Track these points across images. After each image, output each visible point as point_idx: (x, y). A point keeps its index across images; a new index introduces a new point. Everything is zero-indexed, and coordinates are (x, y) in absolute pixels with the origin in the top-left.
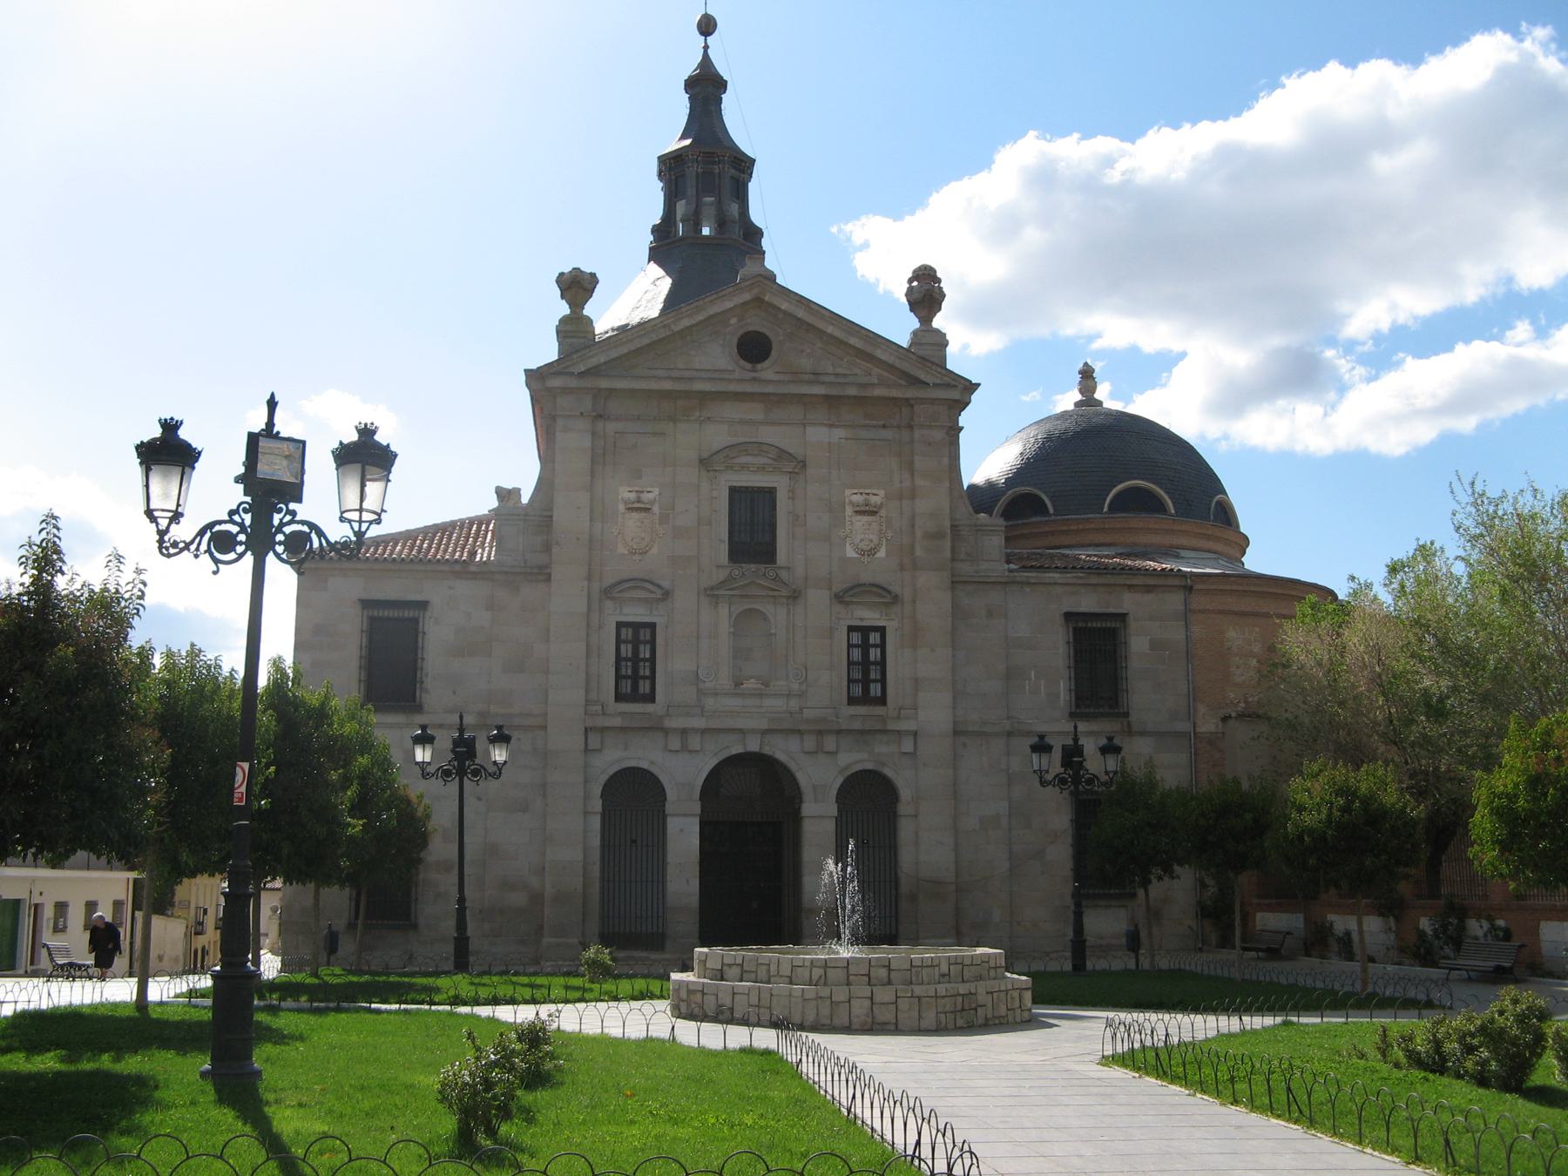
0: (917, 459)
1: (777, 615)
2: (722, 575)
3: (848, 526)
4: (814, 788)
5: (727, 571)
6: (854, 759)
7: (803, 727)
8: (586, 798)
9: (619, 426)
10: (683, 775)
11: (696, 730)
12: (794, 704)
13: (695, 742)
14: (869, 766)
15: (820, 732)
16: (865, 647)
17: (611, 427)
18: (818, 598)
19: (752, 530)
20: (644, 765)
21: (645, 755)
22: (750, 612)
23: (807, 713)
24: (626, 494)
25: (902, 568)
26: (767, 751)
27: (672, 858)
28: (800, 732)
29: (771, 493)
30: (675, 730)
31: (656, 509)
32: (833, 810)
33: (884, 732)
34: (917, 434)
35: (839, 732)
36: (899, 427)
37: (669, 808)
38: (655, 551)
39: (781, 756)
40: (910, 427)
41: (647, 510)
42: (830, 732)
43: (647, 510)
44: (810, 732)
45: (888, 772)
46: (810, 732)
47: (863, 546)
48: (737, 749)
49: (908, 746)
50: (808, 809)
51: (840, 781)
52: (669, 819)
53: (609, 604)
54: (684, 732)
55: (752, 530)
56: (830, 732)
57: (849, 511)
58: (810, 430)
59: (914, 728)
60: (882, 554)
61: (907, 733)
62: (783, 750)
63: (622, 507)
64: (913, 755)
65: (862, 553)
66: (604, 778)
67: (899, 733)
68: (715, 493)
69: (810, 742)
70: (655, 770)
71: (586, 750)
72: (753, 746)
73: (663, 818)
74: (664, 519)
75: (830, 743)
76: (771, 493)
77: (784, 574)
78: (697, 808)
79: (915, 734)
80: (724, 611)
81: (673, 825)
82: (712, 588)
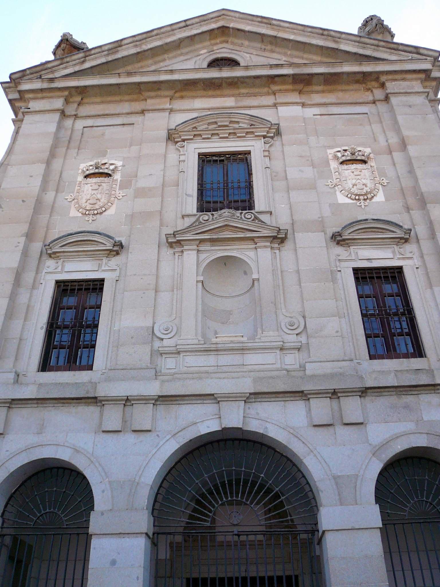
0: (400, 118)
1: (260, 259)
2: (188, 222)
3: (335, 176)
4: (336, 478)
5: (193, 219)
9: (89, 122)
11: (144, 400)
12: (291, 360)
13: (143, 416)
15: (335, 394)
16: (379, 298)
17: (80, 124)
18: (311, 248)
19: (224, 185)
20: (64, 455)
22: (226, 262)
23: (310, 369)
24: (86, 165)
25: (408, 209)
26: (254, 426)
29: (243, 158)
30: (114, 400)
31: (117, 176)
32: (373, 515)
34: (394, 100)
35: (364, 392)
36: (374, 102)
37: (96, 523)
38: (112, 211)
39: (276, 433)
40: (387, 99)
41: (108, 175)
42: (349, 392)
43: (108, 175)
44: (319, 394)
46: (319, 394)
47: (355, 190)
48: (209, 426)
50: (329, 517)
51: (377, 467)
52: (95, 543)
53: (50, 263)
54: (127, 401)
55: (224, 185)
56: (349, 392)
57: (334, 165)
58: (280, 108)
60: (380, 197)
62: (278, 423)
63: (80, 178)
65: (357, 197)
68: (182, 158)
69: (321, 408)
70: (80, 464)
72: (234, 417)
73: (84, 538)
74: (125, 185)
75: (352, 408)
76: (243, 158)
77: (264, 218)
78: (143, 522)
80: (190, 257)
81: (100, 550)
82: (174, 235)
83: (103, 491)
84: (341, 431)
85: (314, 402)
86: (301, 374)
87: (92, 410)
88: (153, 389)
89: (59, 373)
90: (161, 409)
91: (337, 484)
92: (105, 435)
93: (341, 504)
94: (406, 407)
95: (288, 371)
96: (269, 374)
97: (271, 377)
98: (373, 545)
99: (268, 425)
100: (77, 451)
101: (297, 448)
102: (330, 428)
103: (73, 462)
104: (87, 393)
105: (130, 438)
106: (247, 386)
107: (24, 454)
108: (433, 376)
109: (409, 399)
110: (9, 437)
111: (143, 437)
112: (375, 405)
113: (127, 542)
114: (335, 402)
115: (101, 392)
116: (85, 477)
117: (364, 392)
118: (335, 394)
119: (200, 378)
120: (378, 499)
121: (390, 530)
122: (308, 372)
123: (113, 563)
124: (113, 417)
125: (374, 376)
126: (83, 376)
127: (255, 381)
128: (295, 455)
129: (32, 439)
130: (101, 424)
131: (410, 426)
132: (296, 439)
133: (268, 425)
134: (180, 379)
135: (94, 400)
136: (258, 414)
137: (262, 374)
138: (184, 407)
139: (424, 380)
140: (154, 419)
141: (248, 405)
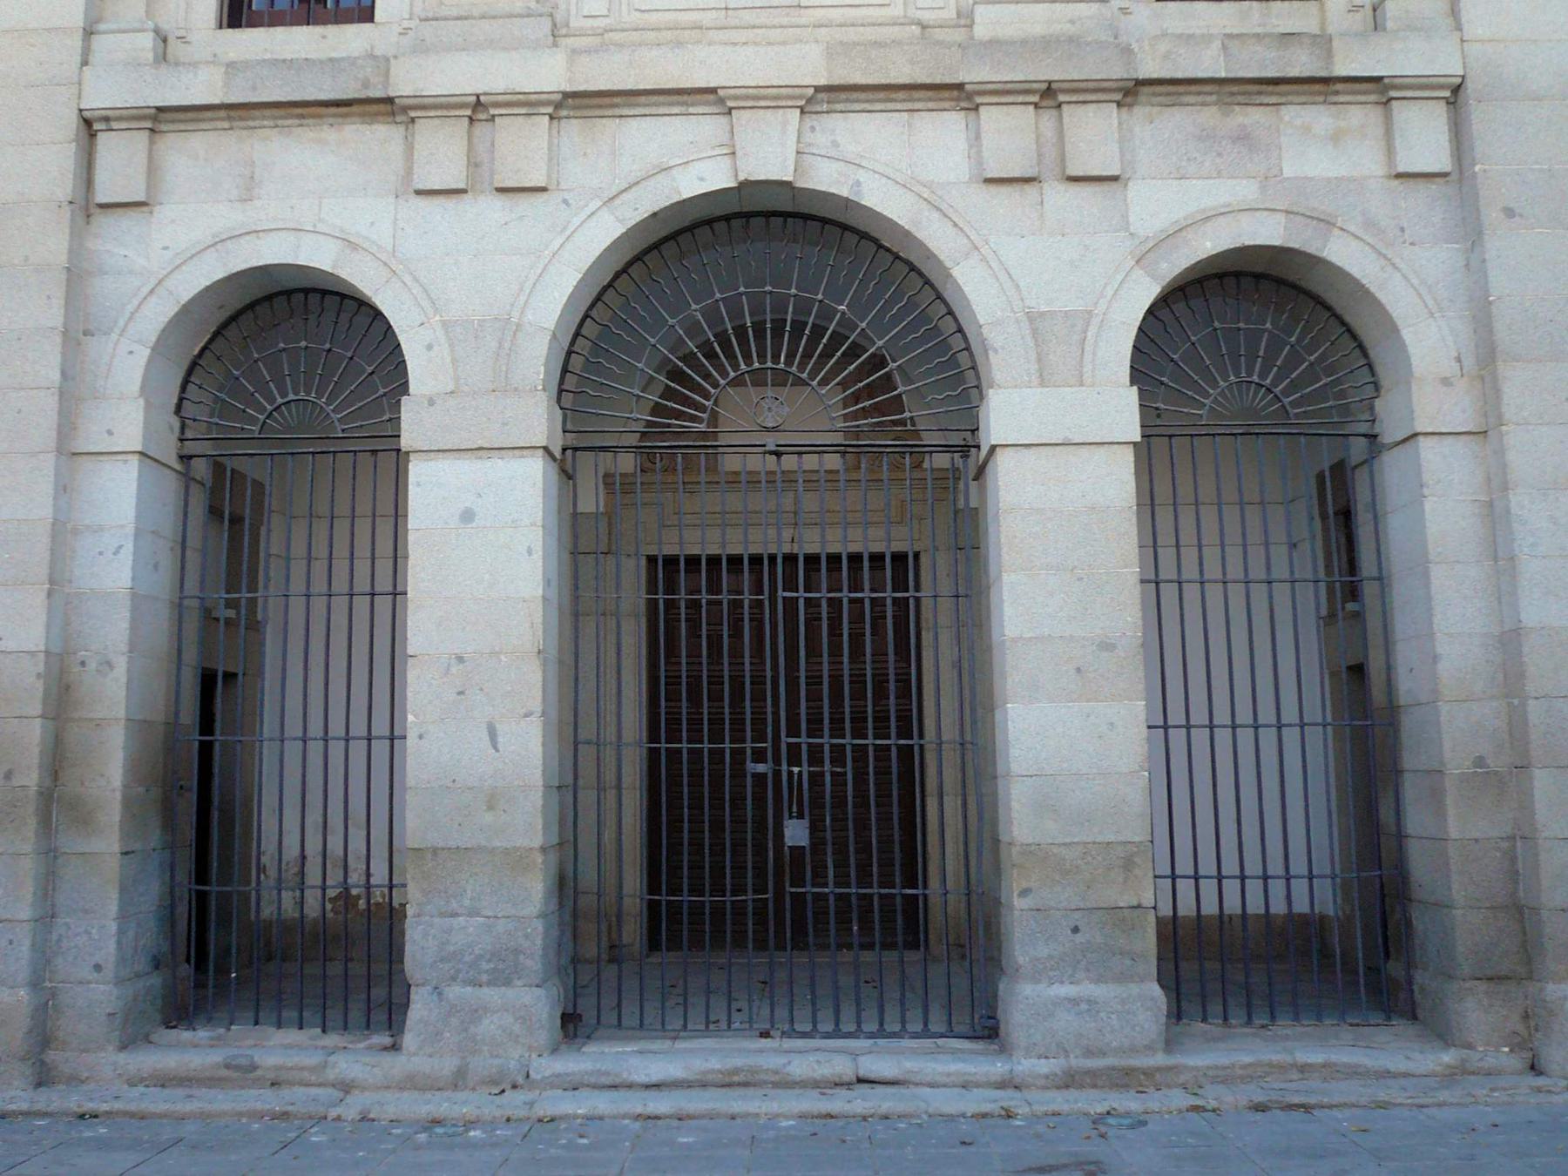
4: (1034, 318)
6: (1197, 199)
7: (974, 73)
8: (72, 394)
10: (482, 288)
11: (526, 104)
13: (522, 147)
14: (1267, 232)
15: (1048, 95)
20: (319, 256)
21: (319, 209)
26: (826, 178)
27: (426, 628)
28: (958, 95)
30: (442, 106)
32: (1121, 412)
33: (1322, 86)
35: (1131, 92)
42: (1089, 91)
44: (1006, 93)
45: (1342, 252)
46: (1006, 93)
49: (1423, 137)
50: (1006, 414)
51: (1146, 292)
52: (418, 472)
56: (1089, 91)
59: (1445, 62)
61: (1420, 88)
64: (1457, 177)
66: (158, 313)
67: (1379, 90)
69: (1009, 134)
71: (88, 207)
72: (770, 153)
75: (1094, 134)
78: (536, 419)
79: (1455, 94)
81: (432, 490)
83: (429, 347)
84: (1058, 196)
85: (991, 117)
86: (958, 35)
87: (381, 137)
88: (549, 73)
89: (279, 32)
90: (573, 130)
91: (1035, 333)
92: (422, 202)
93: (1042, 384)
94: (1243, 138)
95: (924, 27)
96: (870, 34)
97: (877, 44)
98: (1114, 482)
99: (862, 176)
100: (354, 246)
101: (936, 237)
102: (1030, 189)
103: (344, 274)
104: (366, 84)
105: (488, 210)
106: (811, 68)
107: (210, 256)
108: (1329, 54)
109: (1253, 117)
110: (164, 213)
111: (525, 202)
112: (1160, 130)
113: (500, 468)
114: (1047, 119)
115: (405, 82)
116: (378, 314)
117: (1131, 92)
118: (1048, 95)
119: (679, 44)
120: (1140, 373)
121: (1158, 447)
122: (980, 31)
123: (468, 516)
124: (441, 152)
125: (1163, 47)
126: (347, 40)
127: (831, 52)
128: (930, 256)
129: (228, 217)
130: (409, 171)
131: (1244, 191)
132: (936, 215)
133: (862, 176)
134: (620, 46)
135: (385, 108)
136: (835, 144)
137: (852, 34)
138: (634, 123)
139: (1301, 63)
140: (553, 159)
141: (809, 121)
